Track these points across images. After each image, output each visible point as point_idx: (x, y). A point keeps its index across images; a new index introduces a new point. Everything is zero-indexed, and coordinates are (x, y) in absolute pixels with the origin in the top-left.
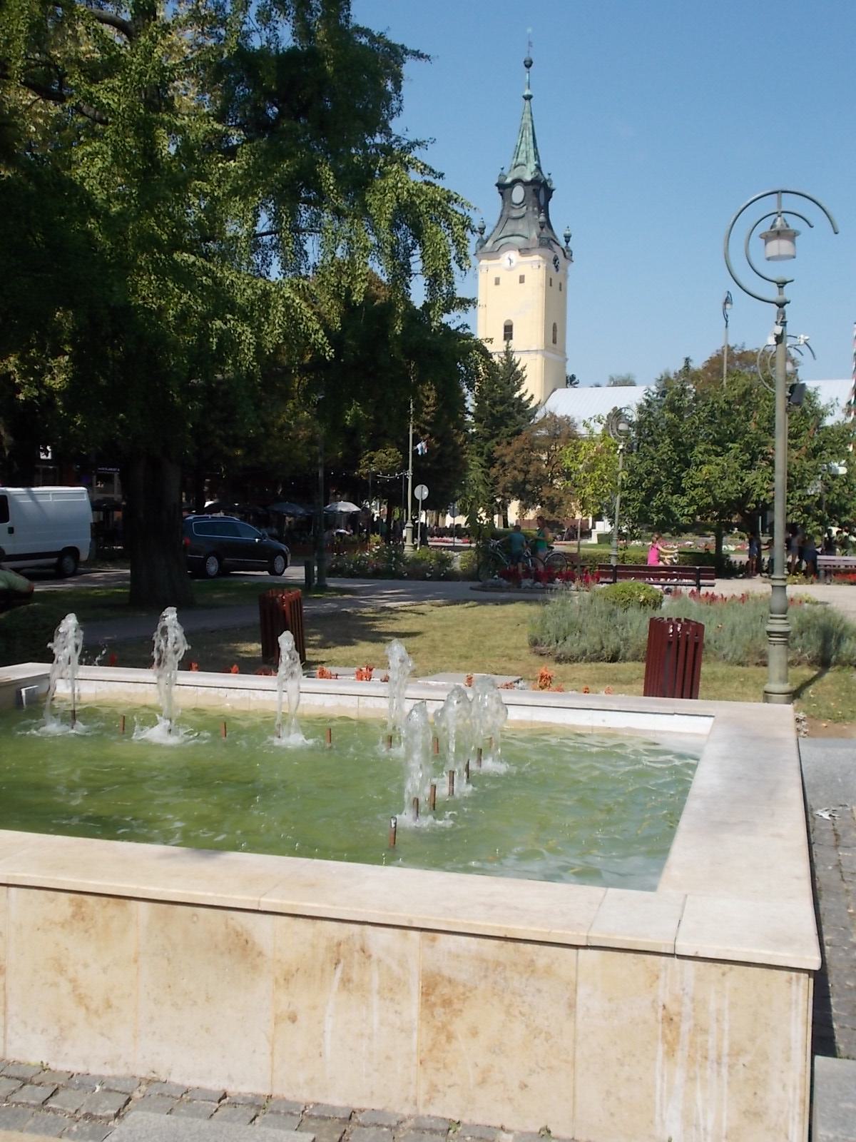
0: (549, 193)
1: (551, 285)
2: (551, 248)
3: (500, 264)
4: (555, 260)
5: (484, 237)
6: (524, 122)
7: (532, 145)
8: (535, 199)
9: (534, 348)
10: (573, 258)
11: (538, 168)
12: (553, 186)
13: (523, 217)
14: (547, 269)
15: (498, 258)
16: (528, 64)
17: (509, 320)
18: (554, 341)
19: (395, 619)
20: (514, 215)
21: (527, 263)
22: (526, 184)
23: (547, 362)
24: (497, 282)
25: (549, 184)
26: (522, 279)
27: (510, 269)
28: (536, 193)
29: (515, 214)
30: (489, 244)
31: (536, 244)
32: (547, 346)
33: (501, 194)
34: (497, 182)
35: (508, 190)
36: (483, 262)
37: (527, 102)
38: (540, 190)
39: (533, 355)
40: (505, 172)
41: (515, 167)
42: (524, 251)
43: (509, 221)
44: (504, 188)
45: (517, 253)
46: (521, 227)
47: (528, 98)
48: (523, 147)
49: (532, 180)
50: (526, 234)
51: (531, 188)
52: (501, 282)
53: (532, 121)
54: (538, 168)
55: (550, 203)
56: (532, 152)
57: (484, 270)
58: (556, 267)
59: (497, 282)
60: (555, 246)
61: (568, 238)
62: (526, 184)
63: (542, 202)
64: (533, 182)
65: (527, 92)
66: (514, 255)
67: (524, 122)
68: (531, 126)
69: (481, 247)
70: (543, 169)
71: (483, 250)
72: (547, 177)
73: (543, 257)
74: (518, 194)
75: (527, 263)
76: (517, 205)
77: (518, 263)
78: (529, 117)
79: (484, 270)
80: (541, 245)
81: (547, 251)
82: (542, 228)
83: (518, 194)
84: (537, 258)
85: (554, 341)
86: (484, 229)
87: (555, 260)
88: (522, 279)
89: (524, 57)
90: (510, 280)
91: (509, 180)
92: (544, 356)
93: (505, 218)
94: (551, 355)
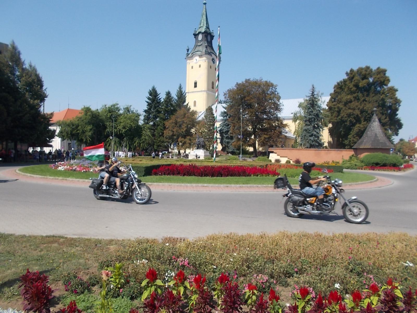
0: (212, 37)
1: (211, 68)
2: (211, 56)
4: (213, 59)
5: (189, 52)
6: (203, 12)
7: (205, 20)
8: (206, 38)
9: (203, 90)
11: (208, 27)
12: (214, 35)
14: (208, 62)
15: (192, 59)
17: (196, 81)
18: (213, 88)
19: (66, 180)
21: (200, 60)
22: (203, 33)
23: (208, 95)
24: (192, 68)
25: (212, 34)
26: (200, 66)
27: (196, 63)
28: (206, 36)
29: (199, 44)
30: (190, 55)
31: (204, 53)
32: (208, 89)
33: (195, 37)
34: (193, 33)
35: (197, 36)
36: (188, 61)
37: (204, 5)
38: (208, 36)
39: (203, 93)
40: (196, 30)
42: (200, 56)
43: (197, 47)
44: (196, 35)
45: (198, 57)
46: (200, 48)
47: (205, 4)
48: (202, 21)
49: (204, 32)
50: (201, 50)
51: (204, 34)
53: (206, 12)
54: (208, 27)
55: (213, 41)
56: (205, 22)
57: (188, 64)
58: (214, 62)
59: (192, 68)
60: (213, 55)
62: (203, 33)
63: (209, 40)
64: (205, 32)
65: (204, 2)
66: (197, 58)
67: (203, 12)
68: (205, 13)
69: (187, 56)
70: (210, 27)
71: (188, 57)
72: (212, 31)
73: (207, 58)
74: (200, 37)
75: (200, 60)
77: (199, 61)
78: (205, 10)
79: (188, 64)
80: (206, 54)
81: (209, 56)
82: (206, 48)
83: (200, 37)
84: (204, 58)
85: (213, 88)
87: (213, 59)
88: (200, 66)
91: (197, 33)
92: (207, 93)
93: (196, 46)
94: (210, 93)
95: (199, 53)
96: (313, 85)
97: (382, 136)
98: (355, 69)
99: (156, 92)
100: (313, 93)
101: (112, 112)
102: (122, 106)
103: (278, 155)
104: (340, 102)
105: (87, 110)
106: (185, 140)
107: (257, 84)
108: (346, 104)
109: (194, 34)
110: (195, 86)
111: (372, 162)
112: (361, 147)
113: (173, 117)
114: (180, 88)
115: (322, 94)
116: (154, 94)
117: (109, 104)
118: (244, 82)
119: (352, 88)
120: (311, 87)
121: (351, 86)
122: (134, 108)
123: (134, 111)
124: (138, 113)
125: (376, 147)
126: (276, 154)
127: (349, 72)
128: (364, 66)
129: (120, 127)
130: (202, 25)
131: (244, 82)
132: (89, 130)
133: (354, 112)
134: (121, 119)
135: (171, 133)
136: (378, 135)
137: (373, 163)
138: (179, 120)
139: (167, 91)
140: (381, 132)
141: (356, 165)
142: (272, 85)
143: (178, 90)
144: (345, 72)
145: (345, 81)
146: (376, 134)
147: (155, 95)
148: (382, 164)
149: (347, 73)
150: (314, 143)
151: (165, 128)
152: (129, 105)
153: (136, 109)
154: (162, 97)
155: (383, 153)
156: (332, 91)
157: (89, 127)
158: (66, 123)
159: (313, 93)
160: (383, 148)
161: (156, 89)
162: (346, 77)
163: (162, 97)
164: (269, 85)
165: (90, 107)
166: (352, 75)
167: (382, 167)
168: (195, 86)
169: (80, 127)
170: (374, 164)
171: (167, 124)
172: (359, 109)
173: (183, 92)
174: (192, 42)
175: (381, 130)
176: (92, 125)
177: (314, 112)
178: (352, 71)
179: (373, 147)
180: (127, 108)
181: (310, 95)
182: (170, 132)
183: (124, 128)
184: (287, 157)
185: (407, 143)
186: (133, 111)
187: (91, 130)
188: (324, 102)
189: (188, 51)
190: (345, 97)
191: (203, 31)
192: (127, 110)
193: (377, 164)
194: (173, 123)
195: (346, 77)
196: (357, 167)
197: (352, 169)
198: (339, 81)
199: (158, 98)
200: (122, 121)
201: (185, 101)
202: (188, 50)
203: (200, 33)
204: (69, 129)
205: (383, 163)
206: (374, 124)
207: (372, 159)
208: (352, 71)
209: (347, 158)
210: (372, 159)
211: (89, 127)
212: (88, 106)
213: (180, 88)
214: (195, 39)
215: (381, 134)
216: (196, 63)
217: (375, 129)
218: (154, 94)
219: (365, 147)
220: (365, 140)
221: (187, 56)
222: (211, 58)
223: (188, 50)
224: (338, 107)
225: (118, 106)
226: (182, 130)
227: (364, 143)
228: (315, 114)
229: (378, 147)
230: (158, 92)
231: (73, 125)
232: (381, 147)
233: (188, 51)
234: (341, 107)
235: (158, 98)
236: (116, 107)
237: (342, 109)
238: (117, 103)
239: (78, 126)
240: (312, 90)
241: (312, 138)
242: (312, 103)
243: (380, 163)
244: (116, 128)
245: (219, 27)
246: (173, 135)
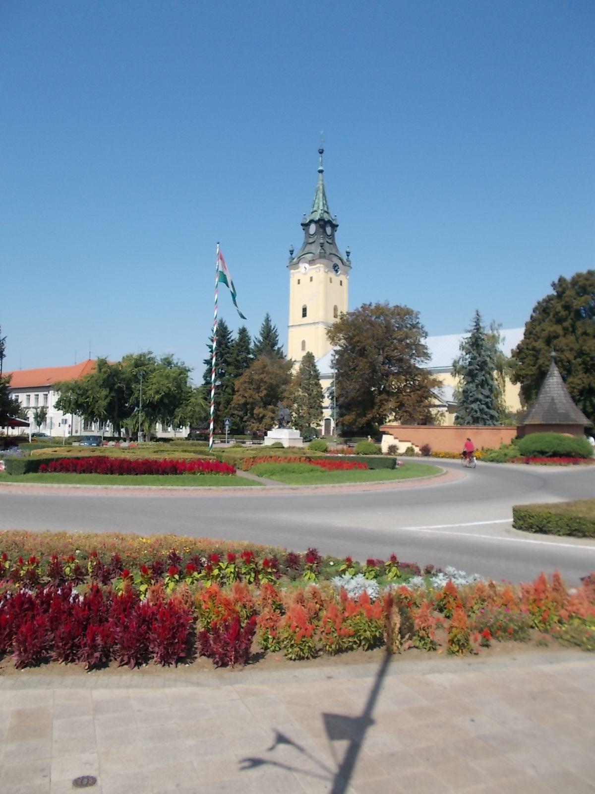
3: (300, 272)
5: (294, 256)
10: (352, 265)
13: (314, 242)
16: (321, 152)
17: (305, 305)
20: (310, 241)
22: (316, 222)
26: (311, 279)
27: (305, 274)
29: (311, 240)
30: (295, 260)
36: (292, 271)
37: (320, 174)
38: (326, 225)
41: (312, 213)
42: (311, 262)
44: (306, 226)
47: (321, 172)
48: (317, 201)
52: (301, 282)
59: (299, 283)
61: (348, 254)
62: (316, 222)
65: (321, 168)
67: (318, 186)
68: (321, 187)
71: (292, 263)
72: (334, 218)
74: (313, 228)
76: (312, 235)
77: (310, 269)
83: (313, 228)
86: (293, 251)
88: (311, 279)
89: (319, 147)
90: (305, 280)
93: (307, 244)
95: (309, 256)
96: (477, 311)
97: (565, 401)
98: (568, 277)
99: (226, 328)
100: (477, 324)
101: (141, 364)
102: (158, 354)
103: (395, 438)
104: (539, 338)
105: (102, 364)
106: (264, 412)
107: (380, 311)
108: (548, 341)
109: (302, 225)
110: (304, 315)
111: (533, 449)
112: (525, 423)
113: (247, 372)
114: (267, 320)
115: (500, 325)
116: (222, 332)
117: (136, 352)
118: (360, 309)
119: (559, 312)
120: (474, 315)
121: (559, 308)
122: (178, 359)
123: (179, 364)
124: (185, 367)
125: (550, 423)
126: (392, 436)
127: (556, 282)
128: (584, 271)
129: (151, 392)
130: (315, 209)
131: (360, 309)
132: (103, 397)
133: (563, 357)
134: (154, 378)
135: (242, 401)
136: (556, 401)
137: (534, 452)
138: (256, 377)
139: (241, 327)
140: (562, 395)
141: (506, 455)
142: (409, 312)
143: (264, 323)
144: (551, 283)
145: (549, 299)
146: (553, 399)
147: (223, 334)
148: (550, 453)
149: (553, 285)
150: (479, 414)
151: (234, 391)
152: (171, 353)
153: (182, 360)
154: (235, 336)
155: (555, 431)
156: (528, 319)
157: (104, 392)
158: (68, 386)
159: (477, 324)
160: (562, 423)
161: (226, 324)
162: (552, 292)
163: (235, 336)
164: (403, 313)
165: (107, 359)
166: (561, 285)
167: (549, 458)
168: (304, 315)
169: (90, 392)
170: (536, 453)
171: (237, 383)
172: (571, 350)
173: (272, 329)
174: (300, 236)
175: (562, 392)
176: (108, 389)
177: (478, 359)
178: (561, 280)
179: (545, 423)
180: (166, 359)
181: (473, 328)
182: (240, 398)
183: (157, 392)
184: (410, 441)
185: (515, 414)
186: (177, 364)
187: (107, 396)
188: (510, 339)
189: (292, 254)
190: (550, 328)
191: (317, 219)
192: (168, 362)
193: (543, 453)
194: (246, 382)
195: (552, 292)
196: (507, 458)
197: (498, 461)
198: (541, 300)
199: (229, 339)
200: (154, 380)
201: (276, 344)
202: (292, 252)
203: (312, 221)
204: (73, 397)
205: (552, 450)
206: (551, 381)
207: (533, 443)
208: (561, 280)
209: (508, 441)
210: (533, 443)
211: (104, 392)
212: (104, 358)
213: (267, 320)
214: (304, 232)
215: (563, 398)
216: (305, 274)
217: (552, 389)
218: (222, 332)
219: (532, 423)
220: (534, 410)
221: (290, 262)
222: (332, 264)
223: (292, 252)
224: (534, 349)
225: (152, 356)
226: (260, 395)
227: (531, 415)
228: (479, 361)
229: (554, 423)
230: (230, 329)
231: (79, 388)
232: (558, 423)
233: (292, 254)
234: (539, 347)
235: (229, 339)
236: (147, 357)
237: (540, 350)
238: (150, 350)
239: (87, 391)
240: (474, 320)
241: (475, 406)
242: (477, 344)
243: (547, 450)
244: (144, 393)
245: (218, 243)
246: (246, 404)
